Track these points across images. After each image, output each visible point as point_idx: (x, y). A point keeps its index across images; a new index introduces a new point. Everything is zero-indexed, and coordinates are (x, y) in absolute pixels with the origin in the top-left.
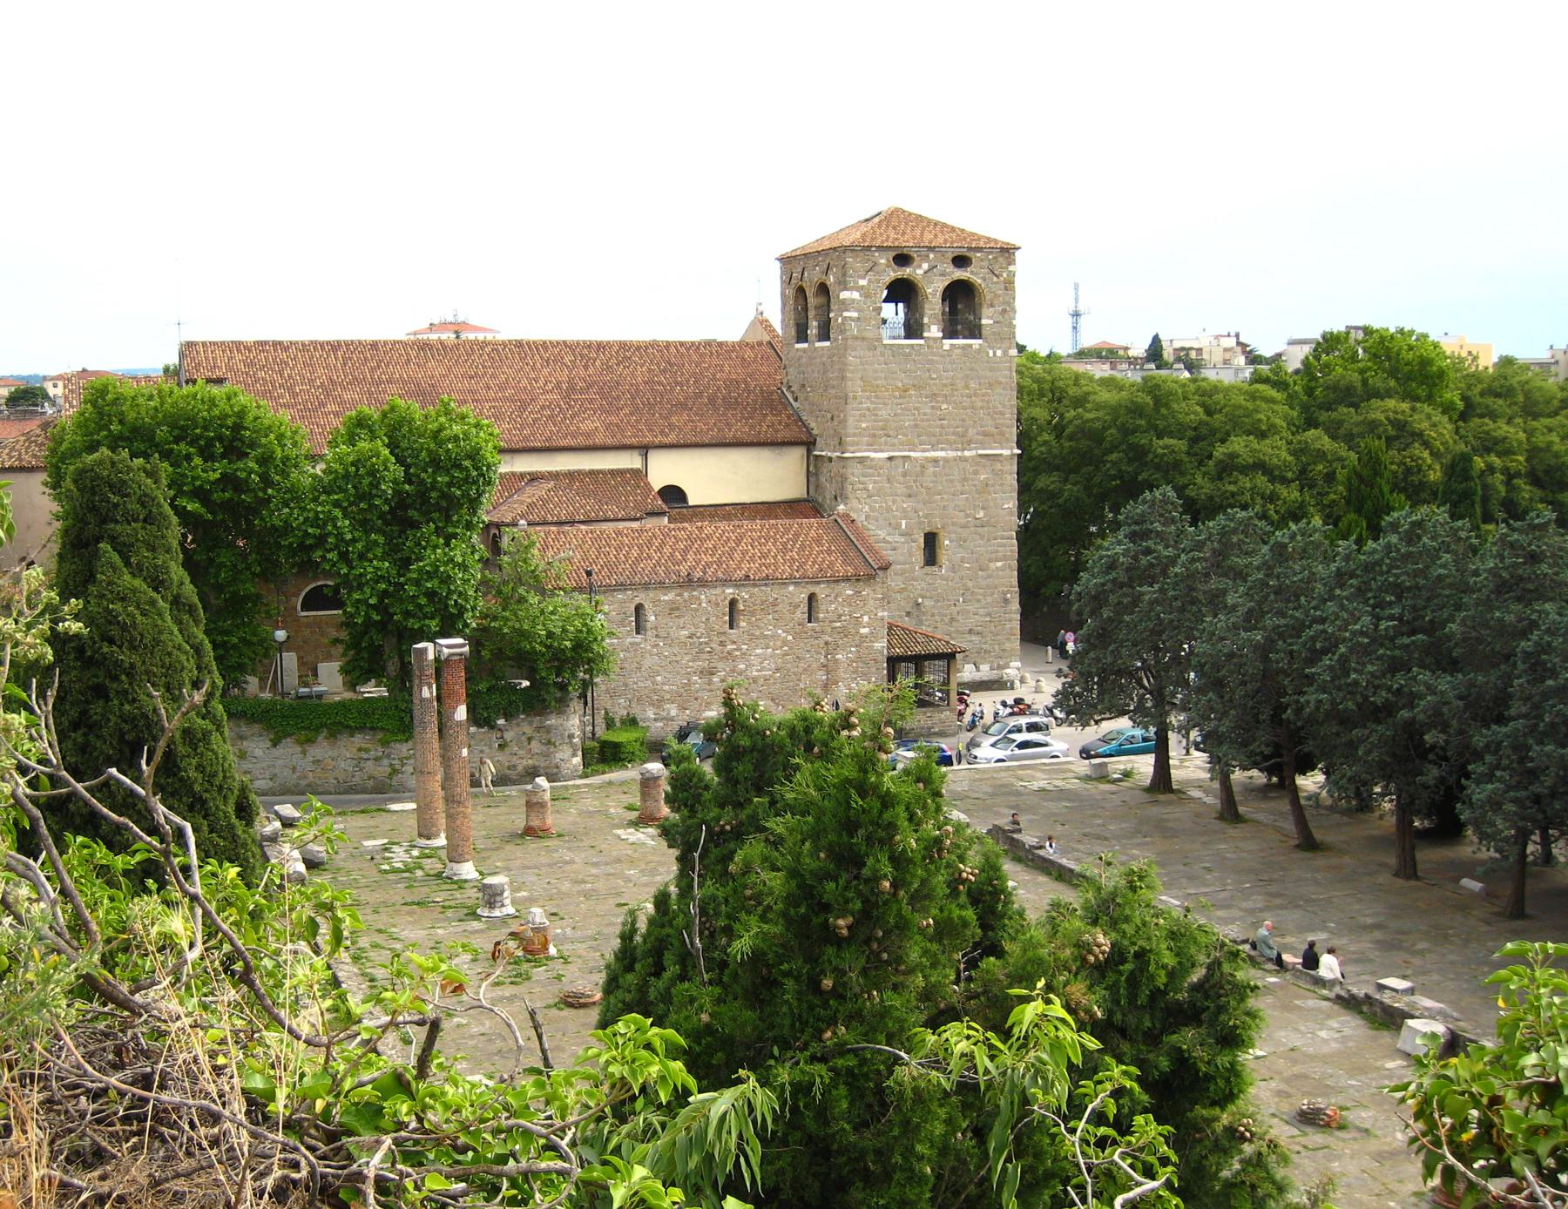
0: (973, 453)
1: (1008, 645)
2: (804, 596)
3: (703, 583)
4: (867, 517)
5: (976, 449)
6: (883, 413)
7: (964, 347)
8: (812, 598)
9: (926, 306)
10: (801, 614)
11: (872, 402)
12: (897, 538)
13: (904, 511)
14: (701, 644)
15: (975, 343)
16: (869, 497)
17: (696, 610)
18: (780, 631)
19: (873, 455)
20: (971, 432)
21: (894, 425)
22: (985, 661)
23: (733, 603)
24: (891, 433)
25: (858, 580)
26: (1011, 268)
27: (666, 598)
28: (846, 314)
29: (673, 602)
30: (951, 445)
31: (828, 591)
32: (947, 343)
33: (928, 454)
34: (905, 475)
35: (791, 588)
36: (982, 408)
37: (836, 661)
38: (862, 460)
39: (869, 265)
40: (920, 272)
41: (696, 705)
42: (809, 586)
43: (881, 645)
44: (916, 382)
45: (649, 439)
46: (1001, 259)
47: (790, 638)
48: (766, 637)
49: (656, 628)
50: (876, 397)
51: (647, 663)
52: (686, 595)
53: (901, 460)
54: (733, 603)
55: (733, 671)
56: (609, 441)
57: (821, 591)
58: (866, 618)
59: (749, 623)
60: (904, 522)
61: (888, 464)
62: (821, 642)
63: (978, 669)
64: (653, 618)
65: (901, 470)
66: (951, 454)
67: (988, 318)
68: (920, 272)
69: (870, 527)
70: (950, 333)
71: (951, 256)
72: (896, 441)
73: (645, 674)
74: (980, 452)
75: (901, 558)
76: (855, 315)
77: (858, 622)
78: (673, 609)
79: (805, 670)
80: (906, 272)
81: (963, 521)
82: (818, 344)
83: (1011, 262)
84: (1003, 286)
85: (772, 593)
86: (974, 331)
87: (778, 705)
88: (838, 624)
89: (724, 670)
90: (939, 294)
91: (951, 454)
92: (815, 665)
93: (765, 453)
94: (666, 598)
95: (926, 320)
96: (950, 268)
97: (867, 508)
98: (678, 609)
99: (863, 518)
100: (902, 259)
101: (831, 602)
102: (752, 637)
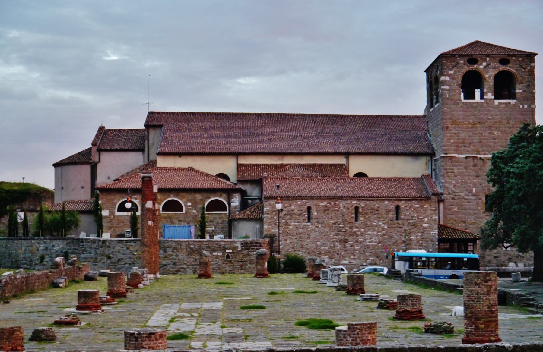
2: (393, 207)
3: (341, 198)
4: (455, 186)
6: (463, 135)
7: (506, 104)
8: (398, 208)
9: (485, 83)
10: (391, 215)
11: (456, 130)
12: (471, 197)
14: (340, 227)
15: (513, 102)
16: (455, 176)
17: (338, 211)
18: (381, 223)
19: (457, 156)
21: (468, 141)
22: (521, 261)
23: (357, 208)
24: (467, 145)
25: (421, 200)
26: (532, 64)
27: (323, 204)
28: (443, 87)
29: (326, 206)
31: (405, 205)
32: (497, 102)
34: (475, 165)
35: (386, 202)
37: (411, 240)
40: (481, 67)
41: (337, 257)
43: (435, 232)
44: (480, 121)
45: (351, 150)
46: (526, 60)
47: (386, 227)
49: (317, 218)
50: (459, 127)
51: (313, 235)
52: (332, 203)
53: (472, 158)
54: (357, 208)
55: (357, 241)
56: (331, 151)
57: (402, 204)
58: (426, 219)
59: (365, 218)
61: (465, 160)
62: (403, 229)
63: (517, 266)
64: (316, 214)
65: (472, 164)
67: (520, 89)
69: (456, 191)
70: (497, 96)
71: (498, 59)
72: (469, 149)
73: (312, 240)
75: (473, 207)
76: (447, 88)
77: (422, 221)
78: (326, 210)
79: (394, 243)
83: (533, 61)
84: (527, 74)
85: (376, 204)
86: (512, 96)
87: (380, 260)
88: (411, 221)
89: (352, 241)
90: (492, 78)
92: (400, 241)
93: (409, 159)
94: (323, 204)
96: (498, 65)
97: (454, 182)
98: (328, 210)
99: (452, 186)
101: (408, 210)
102: (366, 226)
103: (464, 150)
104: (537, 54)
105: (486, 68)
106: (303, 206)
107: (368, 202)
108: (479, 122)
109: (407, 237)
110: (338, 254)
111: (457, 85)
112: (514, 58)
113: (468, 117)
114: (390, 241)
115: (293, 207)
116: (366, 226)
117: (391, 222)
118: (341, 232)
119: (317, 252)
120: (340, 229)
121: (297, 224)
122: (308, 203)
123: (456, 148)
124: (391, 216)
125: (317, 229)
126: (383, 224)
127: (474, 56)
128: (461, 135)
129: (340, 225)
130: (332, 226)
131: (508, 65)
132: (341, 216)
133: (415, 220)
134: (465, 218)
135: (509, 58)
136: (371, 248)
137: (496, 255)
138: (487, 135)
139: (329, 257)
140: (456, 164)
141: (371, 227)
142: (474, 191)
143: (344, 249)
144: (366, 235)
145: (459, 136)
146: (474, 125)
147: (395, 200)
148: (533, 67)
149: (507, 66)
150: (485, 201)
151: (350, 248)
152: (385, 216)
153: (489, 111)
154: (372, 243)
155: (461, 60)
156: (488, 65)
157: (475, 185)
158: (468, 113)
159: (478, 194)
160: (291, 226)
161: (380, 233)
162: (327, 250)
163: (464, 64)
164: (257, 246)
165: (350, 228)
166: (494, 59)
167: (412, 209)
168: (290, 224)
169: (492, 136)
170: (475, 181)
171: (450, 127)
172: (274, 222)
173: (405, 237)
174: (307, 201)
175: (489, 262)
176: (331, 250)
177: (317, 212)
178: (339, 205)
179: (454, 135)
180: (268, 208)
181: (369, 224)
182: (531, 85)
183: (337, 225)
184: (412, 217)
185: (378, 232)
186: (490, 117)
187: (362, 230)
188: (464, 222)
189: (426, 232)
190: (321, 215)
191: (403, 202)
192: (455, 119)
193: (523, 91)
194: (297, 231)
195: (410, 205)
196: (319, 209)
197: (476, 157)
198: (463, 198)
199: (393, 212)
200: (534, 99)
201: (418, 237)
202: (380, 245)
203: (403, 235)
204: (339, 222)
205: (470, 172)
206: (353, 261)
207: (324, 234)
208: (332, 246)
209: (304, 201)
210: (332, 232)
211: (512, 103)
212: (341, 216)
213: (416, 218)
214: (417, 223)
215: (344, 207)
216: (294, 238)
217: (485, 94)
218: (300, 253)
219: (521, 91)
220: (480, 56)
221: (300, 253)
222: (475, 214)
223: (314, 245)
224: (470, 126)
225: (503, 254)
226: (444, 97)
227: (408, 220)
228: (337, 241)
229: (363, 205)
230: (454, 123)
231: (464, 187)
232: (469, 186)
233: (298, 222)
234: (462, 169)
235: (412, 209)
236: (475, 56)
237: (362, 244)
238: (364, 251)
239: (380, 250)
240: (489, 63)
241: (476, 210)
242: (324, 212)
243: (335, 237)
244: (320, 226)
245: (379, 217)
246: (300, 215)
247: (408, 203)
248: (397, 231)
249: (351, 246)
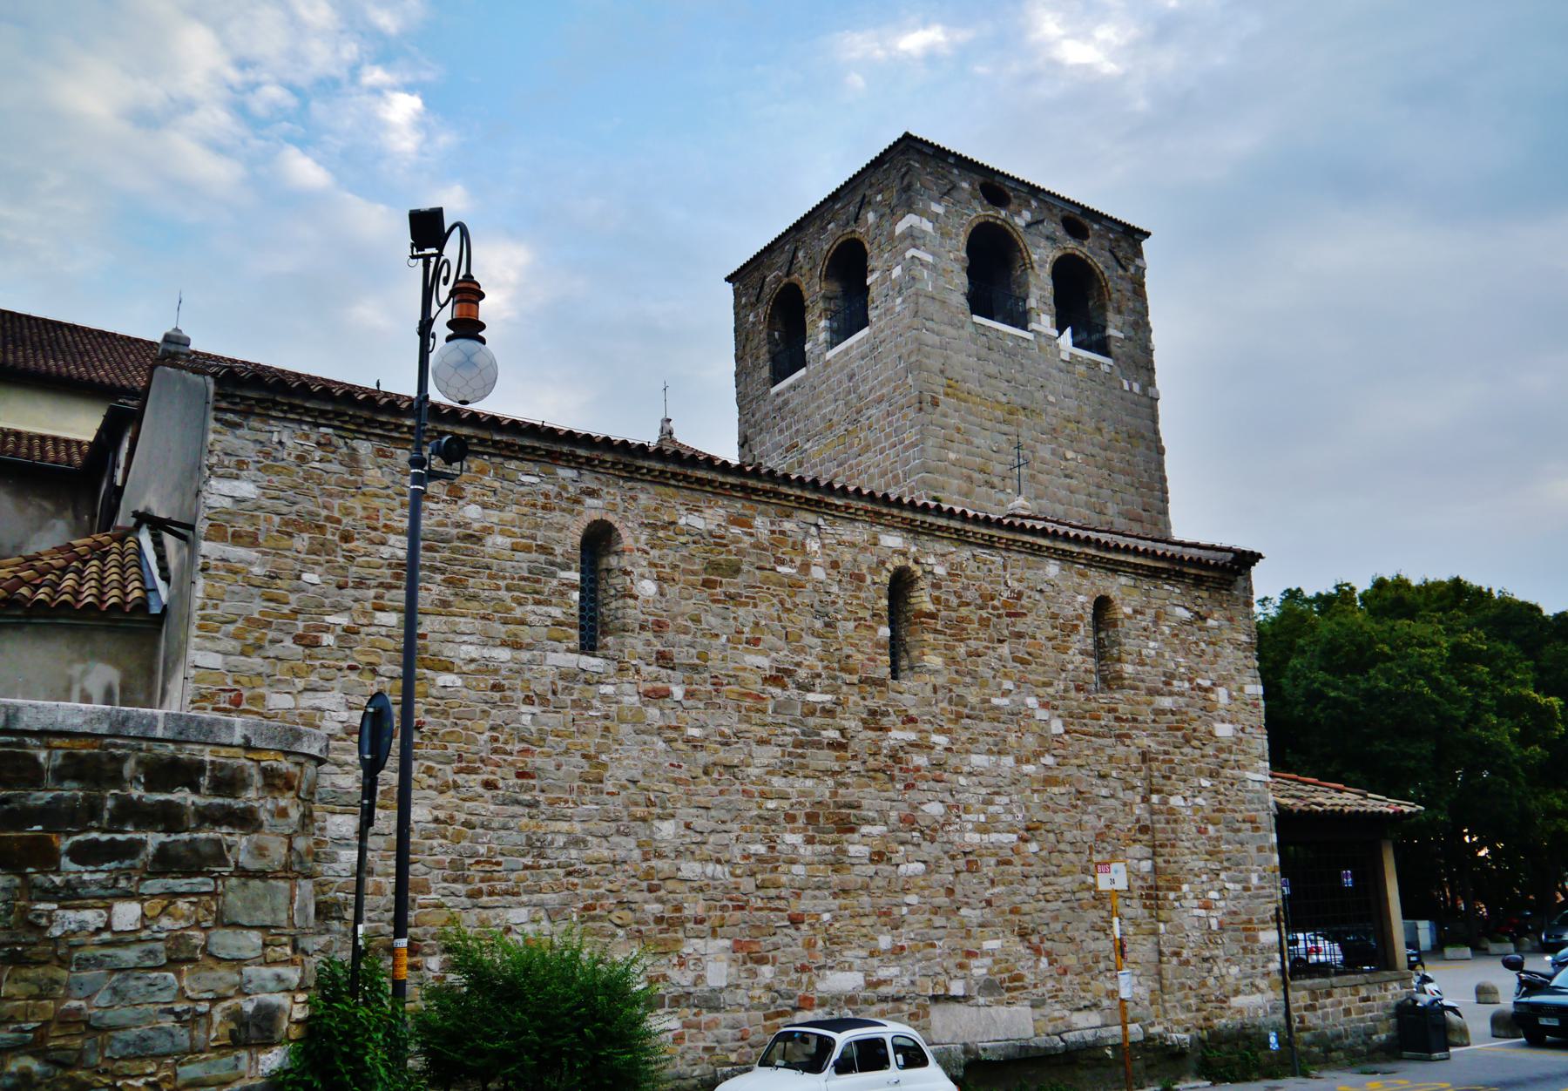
10: (1077, 657)
11: (964, 420)
14: (811, 711)
17: (795, 586)
23: (901, 584)
24: (996, 480)
26: (1138, 262)
27: (697, 522)
29: (718, 541)
35: (1052, 569)
40: (1020, 222)
41: (791, 945)
42: (1092, 573)
44: (1027, 403)
46: (1123, 244)
47: (1057, 727)
48: (995, 714)
49: (659, 627)
52: (761, 524)
54: (901, 584)
55: (909, 821)
58: (1221, 695)
64: (648, 588)
68: (1020, 222)
73: (615, 805)
76: (929, 258)
82: (830, 354)
87: (1037, 951)
88: (1166, 702)
90: (1048, 268)
92: (1124, 823)
94: (697, 522)
95: (1032, 302)
96: (1060, 233)
98: (736, 570)
104: (1147, 235)
105: (1032, 230)
106: (556, 517)
107: (966, 553)
109: (1155, 798)
110: (795, 921)
112: (1096, 227)
113: (993, 381)
114: (1080, 825)
115: (473, 512)
116: (959, 716)
117: (1082, 696)
118: (818, 745)
119: (655, 908)
120: (812, 721)
121: (504, 654)
122: (592, 493)
123: (965, 486)
124: (1079, 658)
125: (653, 712)
126: (1044, 705)
127: (997, 178)
128: (976, 441)
129: (811, 697)
130: (758, 698)
131: (1086, 243)
132: (818, 624)
133: (1182, 694)
135: (1086, 222)
136: (989, 867)
138: (1048, 456)
139: (738, 946)
141: (985, 725)
143: (835, 879)
144: (962, 780)
145: (969, 442)
147: (1091, 562)
148: (1141, 271)
149: (1083, 245)
151: (871, 869)
152: (1050, 656)
154: (994, 837)
158: (991, 369)
160: (448, 668)
161: (1029, 768)
162: (726, 891)
164: (170, 818)
165: (866, 725)
166: (1050, 210)
167: (1167, 630)
168: (448, 651)
169: (1063, 463)
172: (300, 627)
173: (1145, 800)
174: (589, 480)
176: (748, 884)
177: (660, 579)
178: (799, 547)
179: (957, 436)
180: (246, 489)
181: (973, 699)
182: (1140, 325)
183: (793, 692)
184: (1169, 677)
185: (1018, 761)
186: (1051, 398)
187: (941, 740)
189: (1227, 772)
190: (689, 607)
191: (1123, 580)
192: (958, 377)
194: (498, 716)
195: (1156, 603)
196: (672, 557)
199: (1083, 638)
200: (1153, 370)
201: (1199, 800)
202: (1033, 847)
203: (1133, 788)
204: (802, 674)
206: (893, 971)
207: (703, 757)
208: (761, 860)
209: (566, 473)
210: (762, 742)
212: (818, 624)
213: (1187, 685)
214: (1193, 712)
215: (835, 565)
216: (474, 781)
217: (1033, 314)
218: (517, 915)
219: (1121, 335)
221: (517, 915)
223: (627, 848)
224: (998, 413)
226: (919, 286)
227: (1153, 692)
228: (791, 818)
229: (940, 571)
230: (952, 389)
233: (516, 646)
235: (1167, 630)
236: (1002, 180)
237: (941, 837)
238: (950, 892)
239: (1033, 886)
242: (707, 584)
243: (778, 782)
244: (678, 692)
245: (1023, 662)
246: (532, 585)
247: (1147, 594)
248: (1111, 758)
249: (878, 857)
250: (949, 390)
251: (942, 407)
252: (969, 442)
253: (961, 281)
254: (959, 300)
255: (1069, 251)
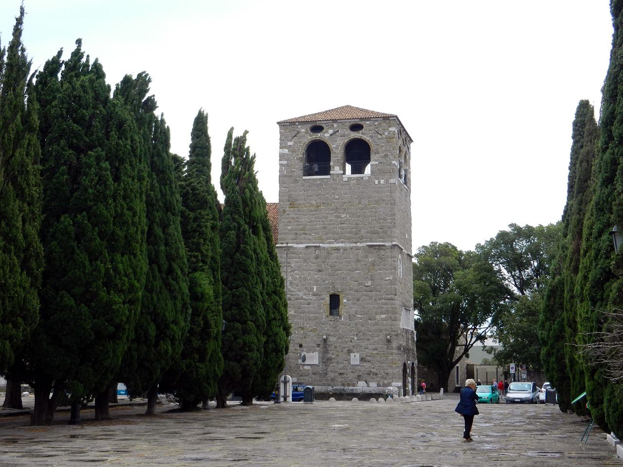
0: (365, 244)
1: (390, 371)
5: (366, 242)
6: (303, 220)
11: (296, 214)
13: (317, 281)
19: (295, 245)
20: (363, 232)
22: (373, 380)
24: (307, 232)
30: (350, 240)
33: (332, 245)
34: (317, 258)
36: (371, 216)
38: (288, 248)
39: (294, 133)
40: (327, 135)
46: (384, 124)
50: (299, 211)
53: (313, 249)
60: (315, 287)
63: (368, 386)
65: (314, 255)
66: (348, 245)
68: (327, 135)
69: (293, 290)
71: (348, 124)
72: (310, 237)
74: (368, 244)
80: (318, 136)
81: (356, 288)
84: (384, 141)
91: (348, 245)
95: (331, 164)
100: (317, 129)
103: (305, 239)
105: (333, 136)
108: (324, 204)
111: (297, 159)
112: (367, 123)
134: (303, 324)
137: (341, 371)
140: (294, 255)
142: (315, 290)
146: (317, 207)
150: (329, 302)
153: (336, 189)
155: (303, 128)
156: (335, 133)
157: (316, 282)
159: (320, 294)
163: (306, 133)
170: (316, 277)
171: (288, 210)
175: (333, 380)
188: (302, 328)
193: (379, 163)
197: (319, 247)
198: (302, 298)
205: (311, 266)
211: (364, 178)
219: (377, 163)
220: (325, 122)
222: (316, 318)
225: (350, 371)
231: (303, 285)
232: (309, 284)
234: (300, 262)
240: (336, 130)
241: (319, 313)
250: (290, 206)
251: (287, 212)
252: (297, 221)
253: (301, 165)
254: (301, 173)
255: (352, 138)
